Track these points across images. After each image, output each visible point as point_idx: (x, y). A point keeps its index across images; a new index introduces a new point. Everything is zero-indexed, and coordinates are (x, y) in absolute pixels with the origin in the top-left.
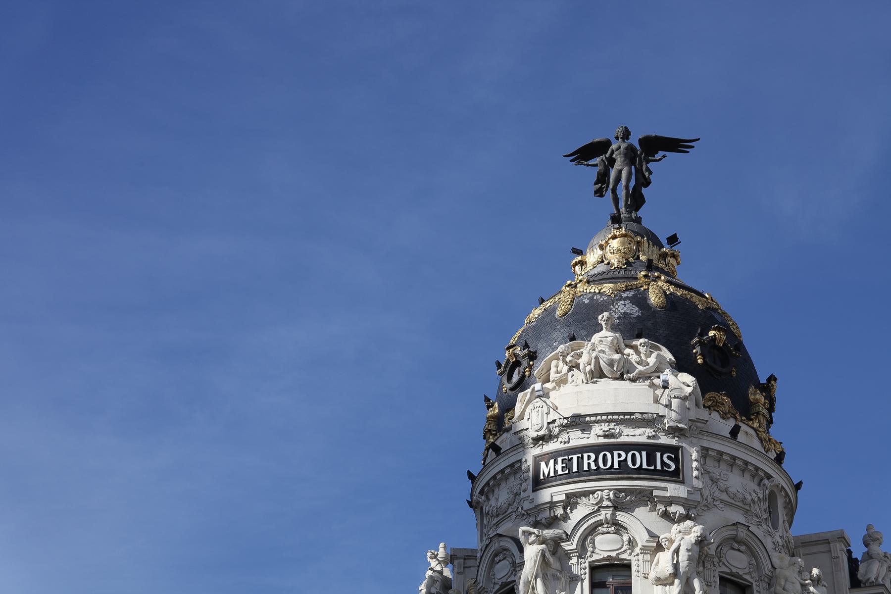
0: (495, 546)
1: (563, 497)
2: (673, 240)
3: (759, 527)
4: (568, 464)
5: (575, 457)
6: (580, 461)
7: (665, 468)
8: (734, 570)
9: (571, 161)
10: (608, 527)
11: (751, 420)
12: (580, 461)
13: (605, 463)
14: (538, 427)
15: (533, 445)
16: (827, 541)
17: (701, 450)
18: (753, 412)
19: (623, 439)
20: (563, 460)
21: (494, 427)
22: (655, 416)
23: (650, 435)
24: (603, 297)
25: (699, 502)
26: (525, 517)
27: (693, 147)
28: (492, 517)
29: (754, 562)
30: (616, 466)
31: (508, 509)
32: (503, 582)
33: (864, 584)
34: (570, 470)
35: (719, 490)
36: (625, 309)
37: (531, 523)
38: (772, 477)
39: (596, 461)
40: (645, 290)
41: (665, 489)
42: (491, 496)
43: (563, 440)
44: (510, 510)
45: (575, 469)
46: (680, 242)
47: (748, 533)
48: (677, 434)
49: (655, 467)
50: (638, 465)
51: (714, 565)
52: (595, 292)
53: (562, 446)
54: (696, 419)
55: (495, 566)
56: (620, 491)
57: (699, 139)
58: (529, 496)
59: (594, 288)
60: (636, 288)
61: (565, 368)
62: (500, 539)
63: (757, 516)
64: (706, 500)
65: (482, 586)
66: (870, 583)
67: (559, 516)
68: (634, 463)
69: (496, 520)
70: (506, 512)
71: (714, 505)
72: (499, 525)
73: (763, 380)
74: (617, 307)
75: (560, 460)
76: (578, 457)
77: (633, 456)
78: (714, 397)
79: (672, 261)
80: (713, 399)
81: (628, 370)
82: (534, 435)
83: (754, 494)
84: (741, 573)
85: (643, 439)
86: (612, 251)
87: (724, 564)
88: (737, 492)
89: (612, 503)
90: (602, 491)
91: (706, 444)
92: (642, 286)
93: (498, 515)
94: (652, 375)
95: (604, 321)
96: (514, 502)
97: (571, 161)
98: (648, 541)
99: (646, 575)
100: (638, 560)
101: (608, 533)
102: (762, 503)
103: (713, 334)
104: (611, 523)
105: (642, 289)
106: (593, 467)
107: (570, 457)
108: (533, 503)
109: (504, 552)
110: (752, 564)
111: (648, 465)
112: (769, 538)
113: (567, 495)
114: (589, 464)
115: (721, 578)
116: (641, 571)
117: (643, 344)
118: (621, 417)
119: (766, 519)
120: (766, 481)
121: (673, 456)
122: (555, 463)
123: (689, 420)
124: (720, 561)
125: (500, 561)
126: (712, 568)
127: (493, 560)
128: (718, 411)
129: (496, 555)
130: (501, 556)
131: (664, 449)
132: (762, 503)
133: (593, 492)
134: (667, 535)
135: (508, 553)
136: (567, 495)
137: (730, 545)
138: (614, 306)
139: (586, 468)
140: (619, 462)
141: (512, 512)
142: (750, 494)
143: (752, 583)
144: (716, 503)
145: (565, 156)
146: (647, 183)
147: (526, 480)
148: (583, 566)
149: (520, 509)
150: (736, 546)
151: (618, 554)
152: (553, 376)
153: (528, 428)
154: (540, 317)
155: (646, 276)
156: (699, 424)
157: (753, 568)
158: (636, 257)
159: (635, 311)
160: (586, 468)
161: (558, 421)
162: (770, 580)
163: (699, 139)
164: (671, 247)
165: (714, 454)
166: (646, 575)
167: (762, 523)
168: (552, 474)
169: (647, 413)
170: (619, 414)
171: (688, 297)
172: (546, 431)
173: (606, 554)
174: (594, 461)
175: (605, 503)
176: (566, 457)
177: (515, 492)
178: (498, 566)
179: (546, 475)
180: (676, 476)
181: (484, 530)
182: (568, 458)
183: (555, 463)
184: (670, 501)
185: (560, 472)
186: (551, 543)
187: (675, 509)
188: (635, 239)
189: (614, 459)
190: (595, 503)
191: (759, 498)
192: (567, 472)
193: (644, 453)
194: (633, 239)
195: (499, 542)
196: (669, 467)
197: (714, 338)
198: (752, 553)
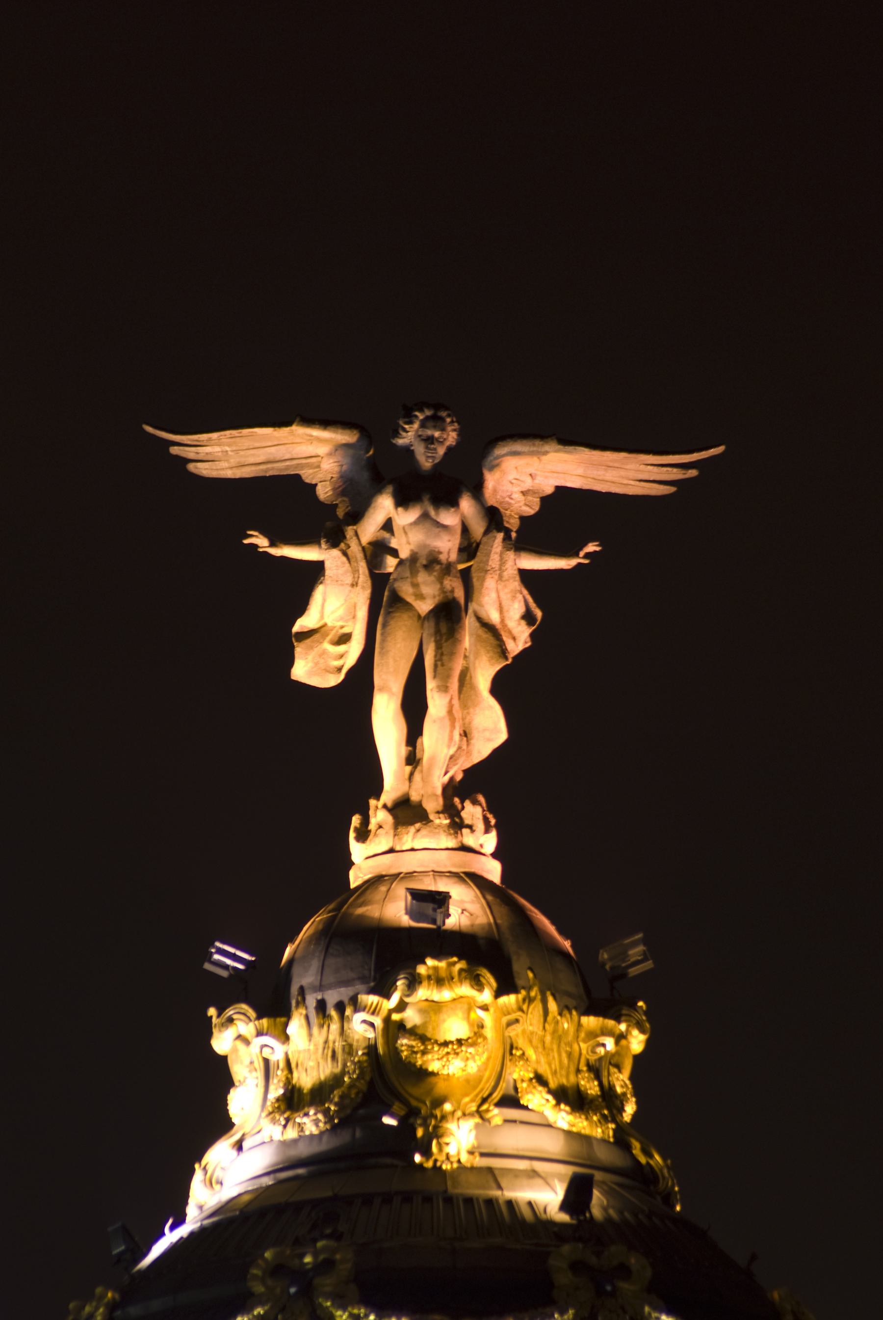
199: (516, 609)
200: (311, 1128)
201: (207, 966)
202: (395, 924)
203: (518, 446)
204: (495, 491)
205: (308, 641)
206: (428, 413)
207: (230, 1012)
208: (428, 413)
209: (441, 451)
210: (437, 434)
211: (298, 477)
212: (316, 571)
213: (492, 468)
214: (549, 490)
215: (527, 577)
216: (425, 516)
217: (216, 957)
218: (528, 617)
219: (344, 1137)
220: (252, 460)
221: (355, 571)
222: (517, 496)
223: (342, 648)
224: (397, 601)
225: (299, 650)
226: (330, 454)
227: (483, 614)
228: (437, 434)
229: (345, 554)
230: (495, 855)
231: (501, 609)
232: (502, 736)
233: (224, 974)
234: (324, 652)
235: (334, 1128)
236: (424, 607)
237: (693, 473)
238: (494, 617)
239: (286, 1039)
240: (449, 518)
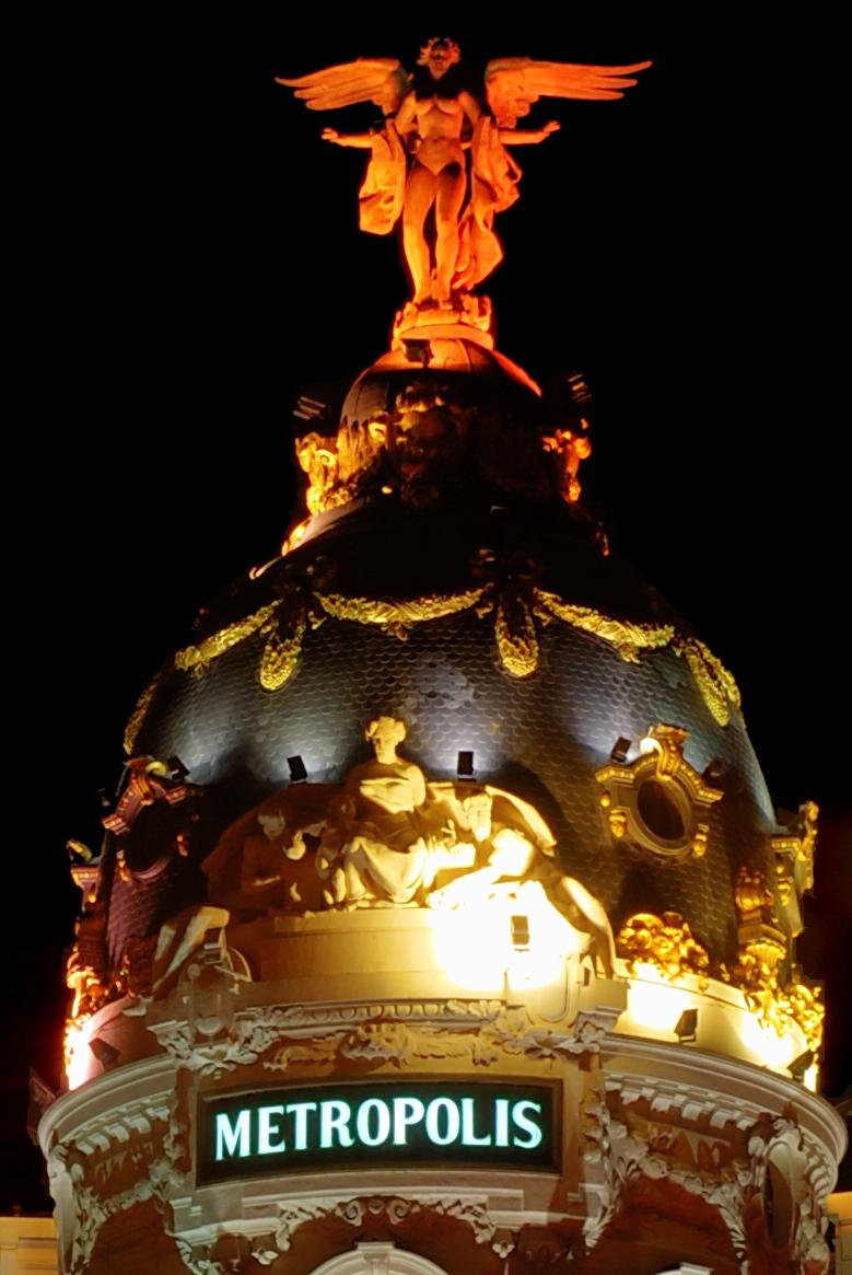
4: (285, 1124)
6: (314, 1120)
7: (518, 1142)
12: (314, 1120)
13: (374, 1131)
30: (400, 1139)
34: (291, 1142)
39: (352, 1125)
45: (301, 1143)
49: (494, 1139)
68: (443, 1132)
76: (310, 1113)
77: (443, 1111)
106: (346, 1141)
111: (479, 1134)
114: (335, 1132)
118: (418, 1008)
121: (537, 1108)
160: (326, 1142)
168: (245, 1152)
169: (477, 1001)
179: (231, 1151)
185: (265, 1148)
192: (281, 1148)
193: (468, 1104)
196: (526, 1136)
199: (502, 169)
200: (341, 502)
201: (296, 413)
202: (403, 367)
203: (503, 64)
204: (496, 98)
205: (368, 202)
206: (437, 40)
207: (306, 440)
208: (437, 40)
209: (446, 65)
210: (442, 53)
211: (370, 102)
212: (365, 155)
213: (490, 81)
214: (535, 99)
215: (512, 150)
216: (435, 107)
217: (303, 407)
218: (511, 175)
219: (360, 503)
220: (342, 93)
221: (392, 151)
222: (513, 104)
223: (390, 205)
224: (419, 166)
225: (363, 208)
226: (387, 82)
227: (479, 174)
228: (442, 53)
229: (385, 138)
230: (490, 331)
231: (493, 173)
232: (498, 257)
233: (307, 418)
234: (380, 210)
235: (355, 499)
236: (437, 169)
237: (633, 83)
238: (487, 176)
239: (335, 451)
240: (449, 107)
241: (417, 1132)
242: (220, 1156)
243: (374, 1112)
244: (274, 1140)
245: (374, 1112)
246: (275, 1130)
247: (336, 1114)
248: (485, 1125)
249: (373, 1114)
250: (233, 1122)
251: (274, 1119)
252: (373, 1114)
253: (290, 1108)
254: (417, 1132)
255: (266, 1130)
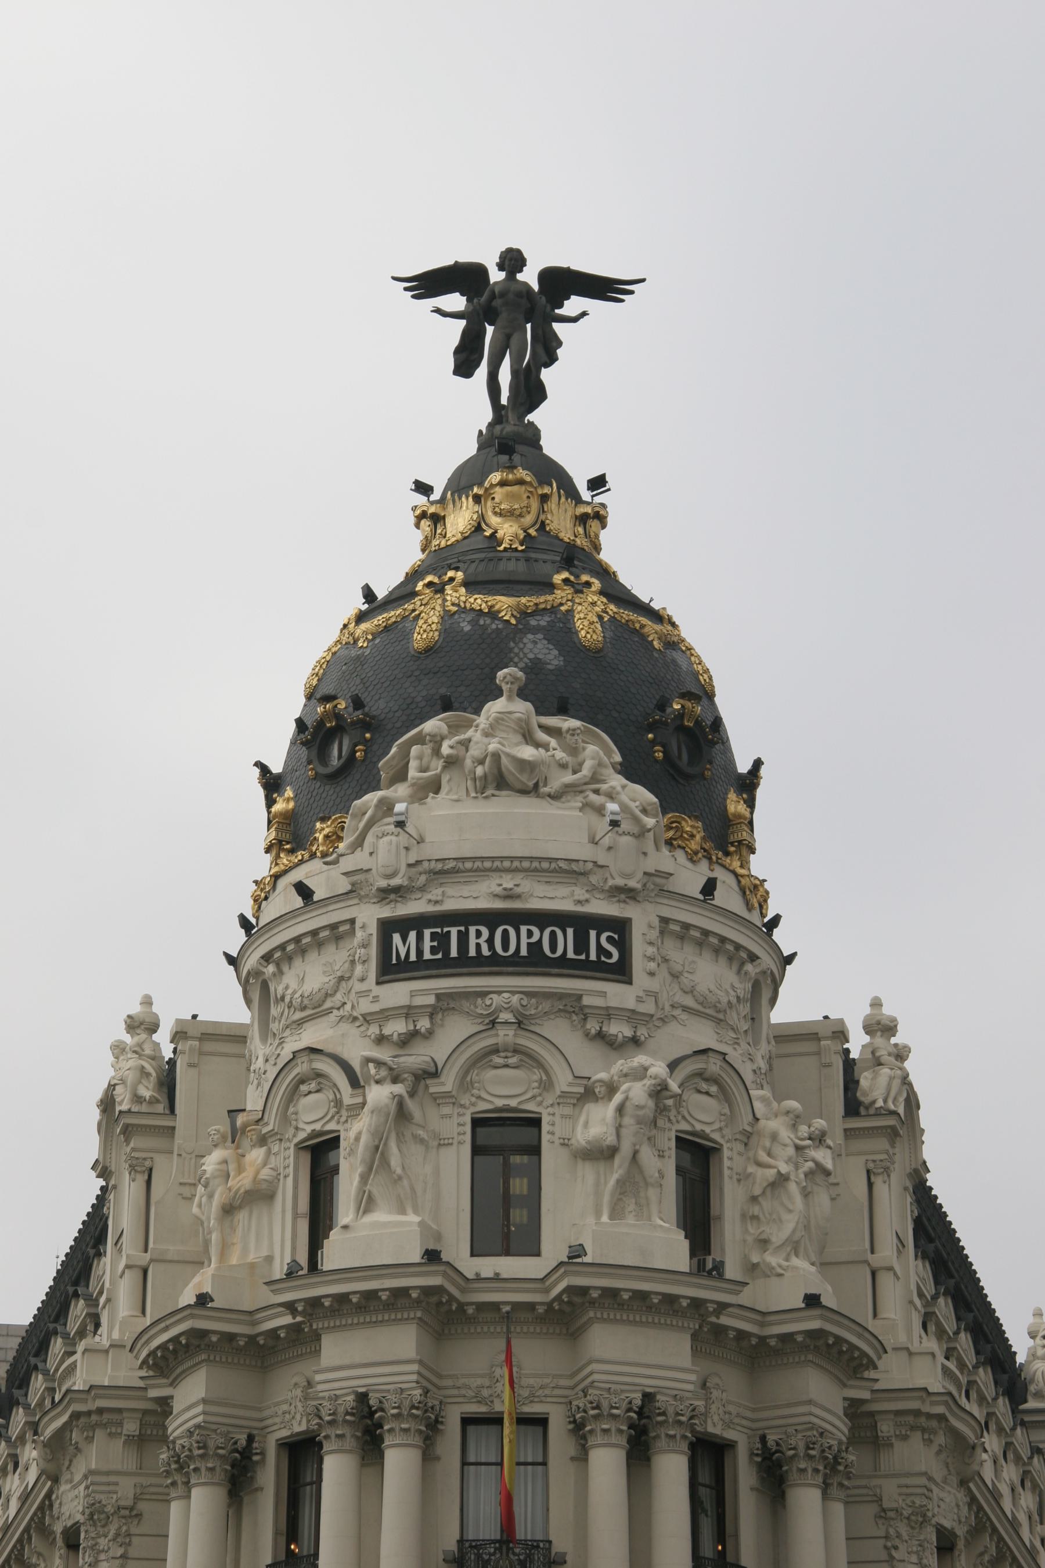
0: (302, 1067)
1: (431, 1000)
2: (598, 483)
3: (736, 1046)
4: (442, 941)
5: (454, 931)
6: (463, 938)
7: (603, 959)
8: (699, 1127)
9: (406, 289)
10: (506, 1057)
11: (727, 854)
12: (463, 938)
13: (505, 946)
14: (389, 871)
15: (375, 900)
16: (815, 1036)
17: (660, 922)
18: (732, 839)
19: (535, 904)
20: (432, 934)
21: (288, 835)
22: (590, 865)
23: (582, 898)
24: (496, 622)
25: (652, 1016)
26: (357, 1024)
27: (632, 292)
28: (289, 1007)
29: (727, 1111)
30: (524, 952)
31: (324, 1001)
32: (314, 1130)
33: (867, 1108)
35: (682, 989)
36: (536, 651)
37: (373, 1036)
38: (758, 958)
39: (490, 941)
40: (568, 611)
41: (603, 994)
42: (285, 968)
43: (434, 898)
44: (328, 1004)
45: (454, 953)
46: (609, 490)
47: (725, 1066)
48: (623, 896)
49: (588, 956)
50: (560, 951)
51: (670, 1120)
52: (481, 610)
53: (431, 908)
54: (656, 871)
55: (298, 1100)
56: (530, 994)
57: (643, 280)
58: (371, 990)
59: (479, 601)
60: (553, 607)
61: (438, 765)
62: (313, 1056)
63: (733, 1029)
64: (663, 1009)
65: (273, 1130)
66: (876, 1109)
67: (423, 1030)
68: (553, 948)
69: (298, 1015)
70: (320, 1006)
71: (673, 1016)
72: (305, 1025)
73: (743, 766)
74: (521, 645)
75: (427, 933)
76: (459, 932)
77: (553, 934)
78: (679, 823)
79: (594, 524)
80: (676, 827)
81: (546, 778)
82: (383, 883)
83: (733, 993)
84: (707, 1130)
85: (566, 906)
86: (497, 509)
87: (684, 1117)
88: (707, 992)
89: (514, 1016)
90: (499, 993)
91: (666, 913)
92: (561, 604)
93: (303, 1008)
94: (585, 787)
95: (507, 683)
96: (336, 992)
97: (406, 289)
98: (570, 1084)
99: (566, 1141)
100: (553, 1114)
101: (506, 1066)
102: (741, 1006)
103: (679, 707)
104: (512, 1049)
105: (563, 608)
106: (485, 951)
107: (446, 930)
108: (377, 1003)
109: (319, 1080)
110: (724, 1115)
111: (577, 952)
112: (749, 1064)
113: (438, 997)
114: (478, 945)
115: (678, 1139)
116: (558, 1134)
117: (571, 732)
119: (746, 1031)
120: (749, 967)
121: (616, 937)
122: (420, 938)
123: (645, 873)
124: (679, 1113)
125: (310, 1092)
126: (668, 1125)
127: (296, 1087)
128: (684, 848)
129: (302, 1081)
130: (313, 1086)
131: (602, 923)
132: (741, 1006)
133: (484, 994)
134: (603, 1075)
135: (325, 1082)
136: (438, 997)
137: (695, 1086)
138: (516, 644)
139: (472, 952)
140: (529, 944)
141: (332, 1008)
142: (727, 993)
143: (722, 1145)
144: (676, 1012)
145: (395, 278)
146: (551, 359)
147: (364, 961)
148: (461, 1120)
149: (348, 1007)
150: (704, 1086)
151: (520, 1103)
152: (413, 773)
153: (370, 870)
154: (377, 641)
155: (566, 581)
156: (658, 880)
157: (724, 1121)
158: (537, 526)
159: (552, 658)
160: (472, 952)
161: (426, 865)
162: (748, 1138)
163: (643, 280)
164: (593, 496)
165: (677, 928)
166: (566, 1141)
167: (740, 1041)
168: (413, 957)
169: (577, 861)
170: (531, 859)
171: (637, 626)
172: (405, 879)
173: (499, 1103)
174: (486, 941)
175: (505, 1016)
176: (439, 930)
177: (339, 974)
178: (305, 1101)
179: (403, 956)
180: (622, 972)
181: (271, 1026)
182: (442, 931)
183: (420, 938)
184: (608, 1014)
185: (427, 955)
186: (409, 1079)
187: (619, 1029)
188: (540, 492)
189: (521, 940)
190: (485, 1013)
191: (738, 997)
192: (439, 956)
193: (570, 931)
194: (536, 488)
195: (311, 1061)
196: (609, 955)
197: (681, 715)
198: (725, 1095)
241: (535, 948)
242: (394, 961)
243: (505, 933)
244: (434, 950)
245: (505, 933)
246: (435, 944)
247: (479, 934)
248: (581, 945)
249: (505, 934)
250: (404, 939)
251: (434, 937)
252: (505, 934)
253: (446, 930)
254: (535, 948)
255: (427, 944)
